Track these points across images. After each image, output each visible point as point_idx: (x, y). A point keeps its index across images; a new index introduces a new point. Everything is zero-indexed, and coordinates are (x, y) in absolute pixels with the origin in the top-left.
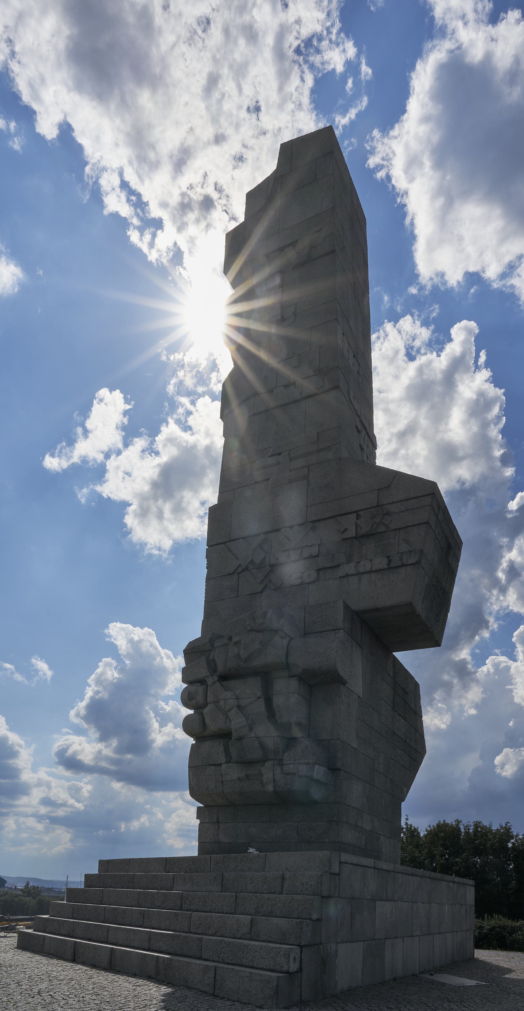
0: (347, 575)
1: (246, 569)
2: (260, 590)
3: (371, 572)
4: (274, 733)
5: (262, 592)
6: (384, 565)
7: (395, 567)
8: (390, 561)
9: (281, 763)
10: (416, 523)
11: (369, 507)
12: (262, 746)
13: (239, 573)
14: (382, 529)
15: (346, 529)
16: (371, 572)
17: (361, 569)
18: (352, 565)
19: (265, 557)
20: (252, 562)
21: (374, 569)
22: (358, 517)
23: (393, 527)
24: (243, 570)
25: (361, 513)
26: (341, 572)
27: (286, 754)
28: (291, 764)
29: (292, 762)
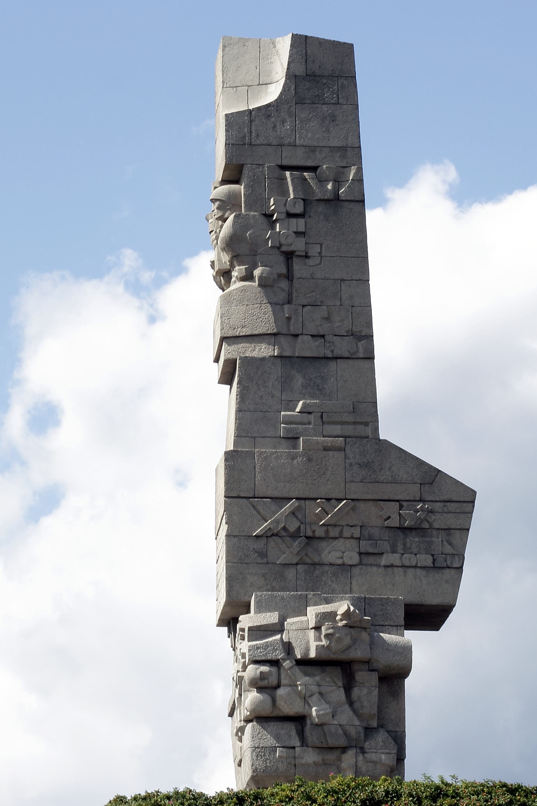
0: (392, 566)
1: (277, 535)
2: (295, 562)
3: (416, 567)
4: (357, 722)
5: (297, 564)
6: (429, 562)
7: (440, 568)
8: (434, 560)
9: (363, 751)
10: (459, 527)
11: (412, 499)
12: (346, 734)
13: (267, 537)
14: (426, 525)
15: (389, 517)
16: (416, 567)
17: (407, 563)
18: (397, 556)
19: (299, 527)
20: (284, 528)
21: (419, 565)
22: (401, 507)
23: (436, 525)
24: (273, 535)
25: (404, 504)
26: (384, 561)
27: (367, 743)
28: (374, 752)
29: (374, 751)
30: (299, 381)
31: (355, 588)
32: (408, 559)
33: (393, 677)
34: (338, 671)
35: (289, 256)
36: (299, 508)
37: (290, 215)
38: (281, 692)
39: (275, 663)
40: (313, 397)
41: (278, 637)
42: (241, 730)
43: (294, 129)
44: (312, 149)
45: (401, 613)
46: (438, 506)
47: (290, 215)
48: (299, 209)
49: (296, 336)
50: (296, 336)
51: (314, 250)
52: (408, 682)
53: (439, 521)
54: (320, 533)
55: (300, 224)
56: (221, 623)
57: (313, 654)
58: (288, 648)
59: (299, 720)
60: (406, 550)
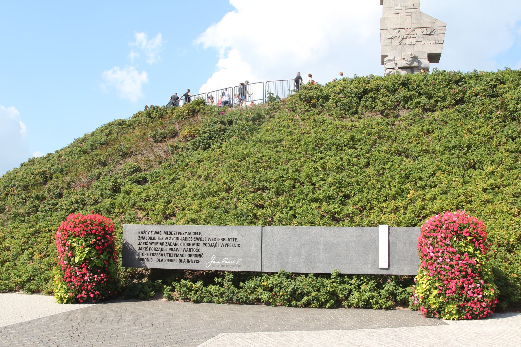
26: (422, 43)
34: (409, 70)
36: (400, 31)
39: (393, 69)
58: (396, 64)
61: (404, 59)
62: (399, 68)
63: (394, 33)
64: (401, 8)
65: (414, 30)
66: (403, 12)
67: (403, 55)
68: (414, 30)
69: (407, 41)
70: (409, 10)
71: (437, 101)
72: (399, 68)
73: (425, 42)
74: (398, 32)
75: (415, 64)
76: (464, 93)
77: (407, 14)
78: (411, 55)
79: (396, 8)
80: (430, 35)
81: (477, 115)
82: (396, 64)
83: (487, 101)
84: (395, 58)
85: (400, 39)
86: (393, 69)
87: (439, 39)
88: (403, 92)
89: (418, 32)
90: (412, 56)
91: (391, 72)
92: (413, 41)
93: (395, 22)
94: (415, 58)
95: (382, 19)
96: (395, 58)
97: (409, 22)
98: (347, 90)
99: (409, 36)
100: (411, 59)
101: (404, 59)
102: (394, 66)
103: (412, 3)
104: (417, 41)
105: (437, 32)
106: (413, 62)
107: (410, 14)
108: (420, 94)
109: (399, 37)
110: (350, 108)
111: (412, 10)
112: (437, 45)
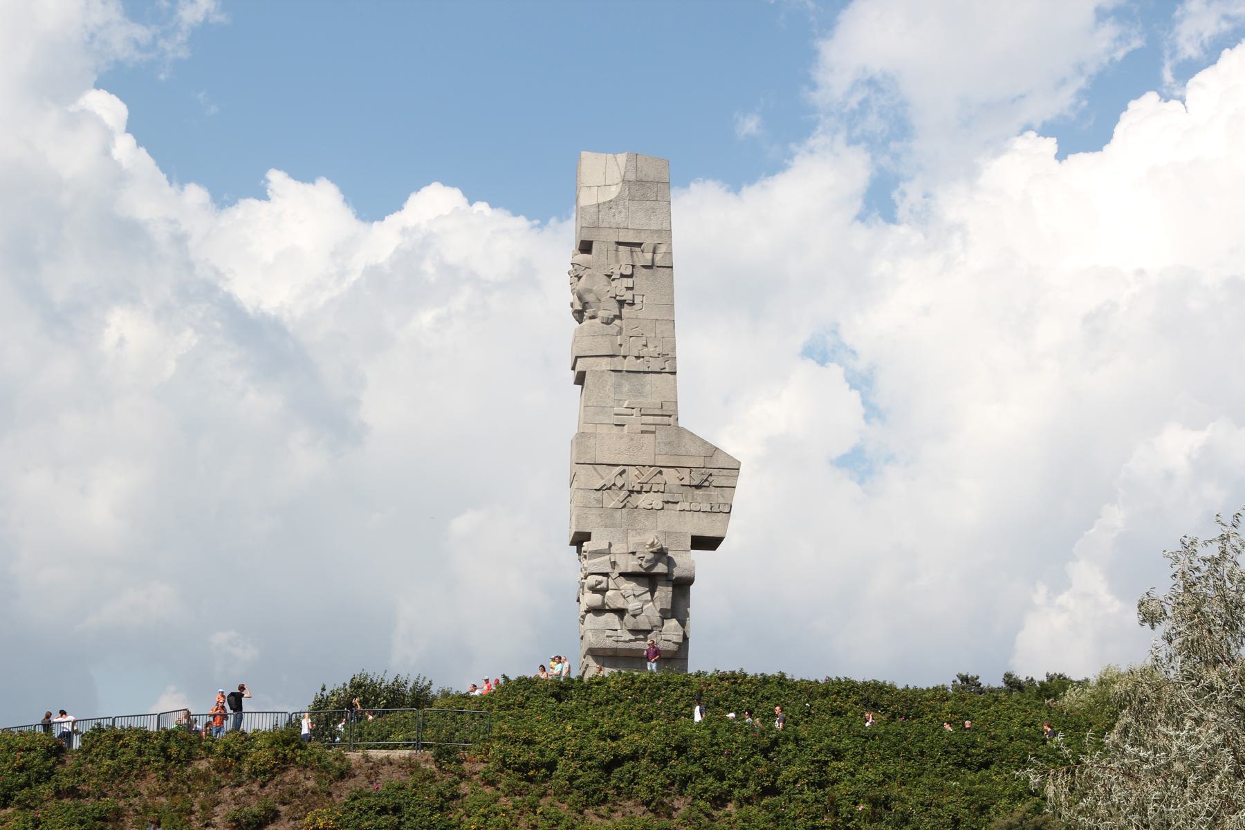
14: (706, 484)
26: (678, 507)
30: (626, 388)
31: (659, 524)
32: (694, 507)
33: (682, 586)
34: (646, 581)
35: (622, 303)
36: (624, 471)
37: (622, 276)
38: (608, 593)
39: (606, 575)
40: (635, 397)
41: (607, 557)
42: (583, 617)
43: (627, 217)
44: (639, 231)
45: (689, 543)
46: (714, 472)
47: (622, 276)
48: (629, 272)
49: (625, 357)
50: (625, 357)
51: (638, 300)
52: (693, 588)
53: (716, 481)
54: (637, 488)
55: (628, 282)
56: (572, 544)
57: (630, 570)
58: (614, 564)
59: (621, 612)
60: (694, 500)
61: (634, 553)
62: (621, 574)
63: (611, 475)
64: (629, 411)
65: (660, 472)
66: (635, 423)
67: (634, 540)
68: (660, 472)
69: (643, 500)
70: (650, 419)
71: (734, 786)
72: (621, 574)
73: (686, 506)
74: (621, 474)
75: (661, 568)
76: (777, 774)
77: (645, 428)
78: (652, 545)
79: (617, 410)
80: (698, 487)
81: (795, 819)
82: (614, 564)
83: (809, 795)
84: (610, 545)
85: (623, 494)
86: (606, 575)
87: (721, 500)
88: (679, 766)
89: (670, 476)
90: (654, 549)
91: (600, 583)
92: (656, 500)
93: (613, 447)
94: (661, 554)
95: (581, 437)
96: (610, 545)
97: (649, 450)
98: (585, 753)
99: (646, 488)
100: (651, 556)
101: (634, 553)
102: (608, 569)
103: (658, 401)
104: (667, 502)
105: (716, 481)
106: (655, 562)
107: (652, 428)
108: (706, 770)
109: (621, 488)
110: (595, 792)
111: (658, 420)
112: (715, 517)
